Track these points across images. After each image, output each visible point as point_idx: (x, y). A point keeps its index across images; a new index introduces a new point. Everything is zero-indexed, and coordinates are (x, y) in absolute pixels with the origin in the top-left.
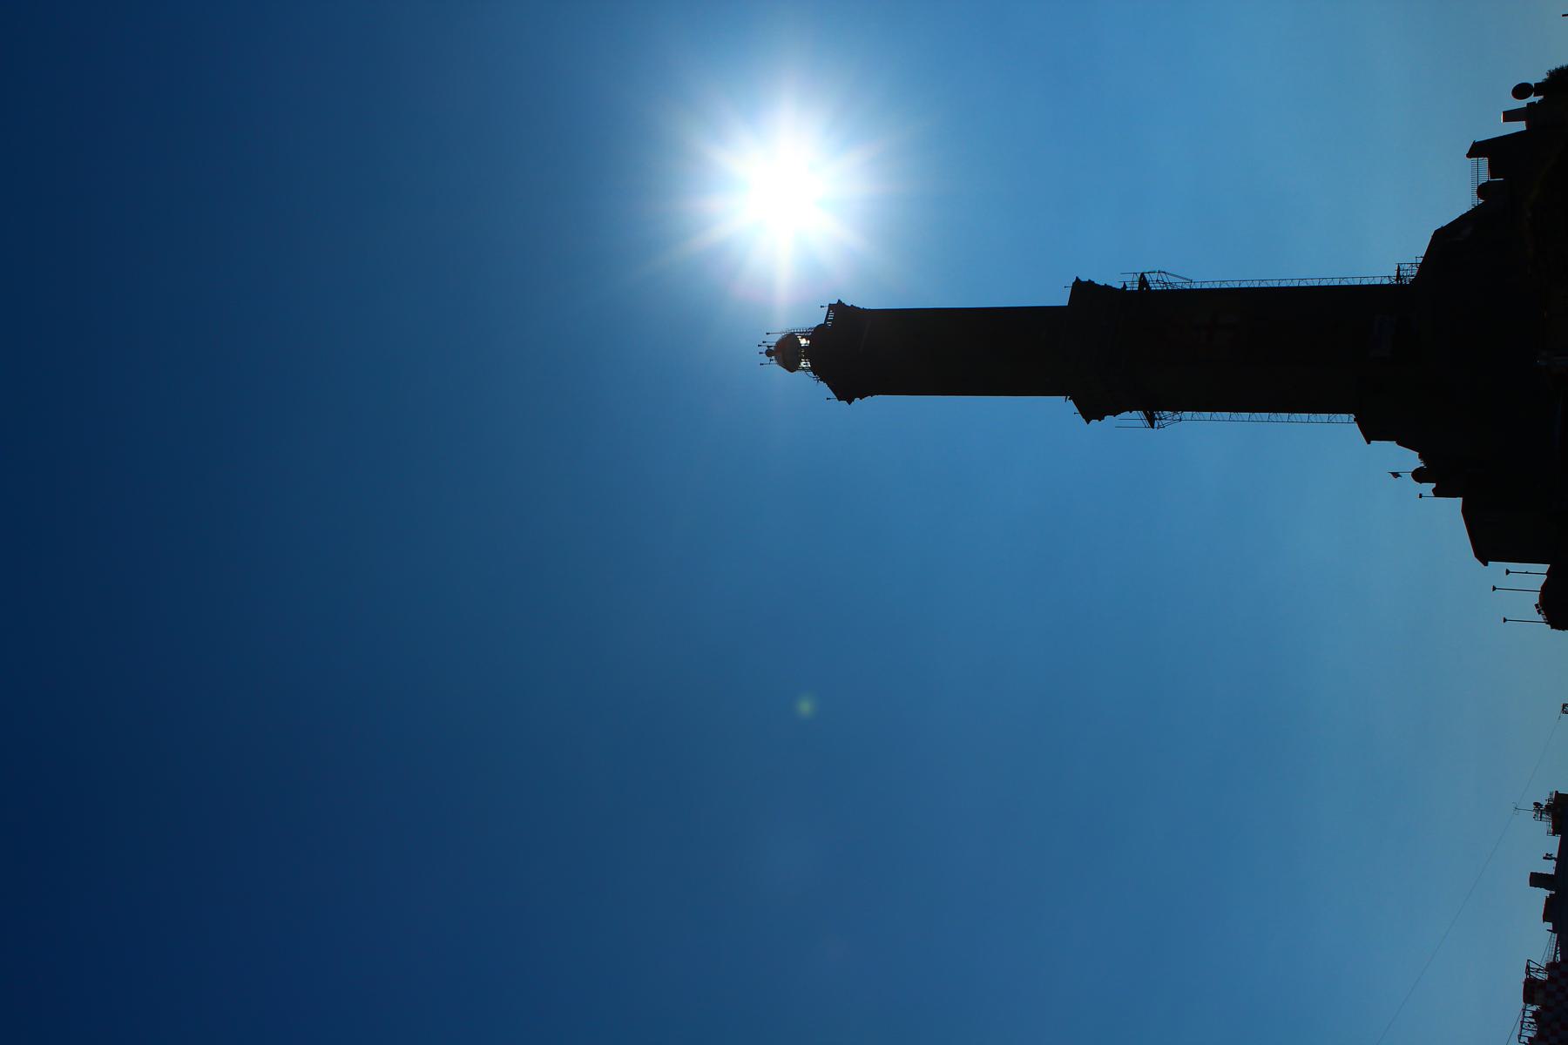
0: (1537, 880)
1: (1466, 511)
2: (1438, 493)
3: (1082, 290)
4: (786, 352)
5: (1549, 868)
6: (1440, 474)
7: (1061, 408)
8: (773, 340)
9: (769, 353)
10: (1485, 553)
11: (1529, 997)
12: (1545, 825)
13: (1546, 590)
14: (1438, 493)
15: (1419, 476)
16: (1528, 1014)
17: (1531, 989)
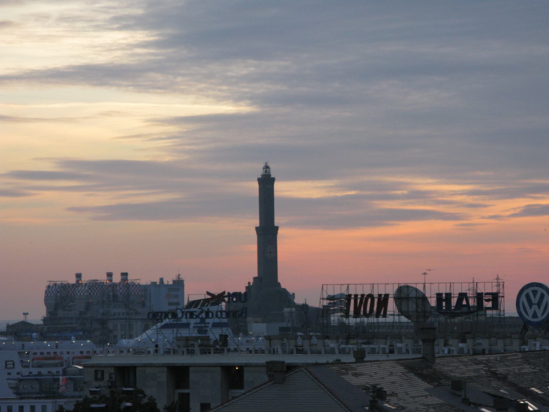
0: (162, 280)
5: (165, 283)
8: (269, 165)
12: (175, 278)
15: (249, 283)
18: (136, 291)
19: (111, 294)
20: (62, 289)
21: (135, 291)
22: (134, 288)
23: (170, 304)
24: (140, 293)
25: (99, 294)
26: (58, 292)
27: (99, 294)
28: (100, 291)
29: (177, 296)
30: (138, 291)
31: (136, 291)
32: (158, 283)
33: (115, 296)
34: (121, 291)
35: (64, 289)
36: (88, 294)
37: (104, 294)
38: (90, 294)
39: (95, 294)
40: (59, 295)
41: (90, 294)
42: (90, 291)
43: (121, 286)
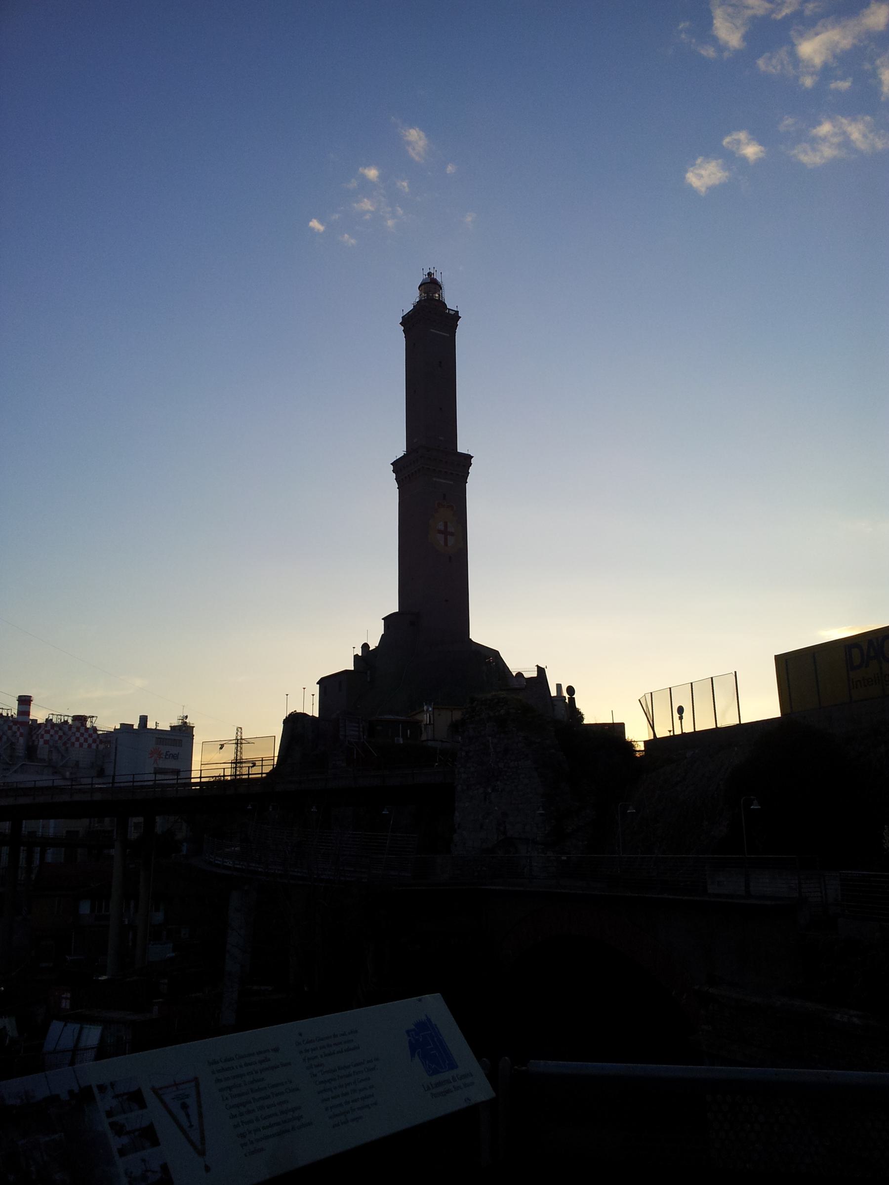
0: (144, 719)
1: (346, 672)
2: (356, 656)
3: (467, 459)
4: (431, 286)
5: (151, 725)
6: (366, 659)
7: (399, 449)
9: (429, 274)
10: (322, 682)
11: (76, 718)
12: (176, 722)
13: (304, 715)
14: (356, 656)
15: (365, 646)
16: (66, 718)
17: (80, 720)
18: (86, 740)
19: (21, 740)
21: (82, 740)
22: (82, 735)
23: (157, 771)
24: (94, 746)
29: (175, 757)
31: (86, 740)
32: (136, 727)
33: (31, 751)
34: (47, 737)
43: (49, 728)
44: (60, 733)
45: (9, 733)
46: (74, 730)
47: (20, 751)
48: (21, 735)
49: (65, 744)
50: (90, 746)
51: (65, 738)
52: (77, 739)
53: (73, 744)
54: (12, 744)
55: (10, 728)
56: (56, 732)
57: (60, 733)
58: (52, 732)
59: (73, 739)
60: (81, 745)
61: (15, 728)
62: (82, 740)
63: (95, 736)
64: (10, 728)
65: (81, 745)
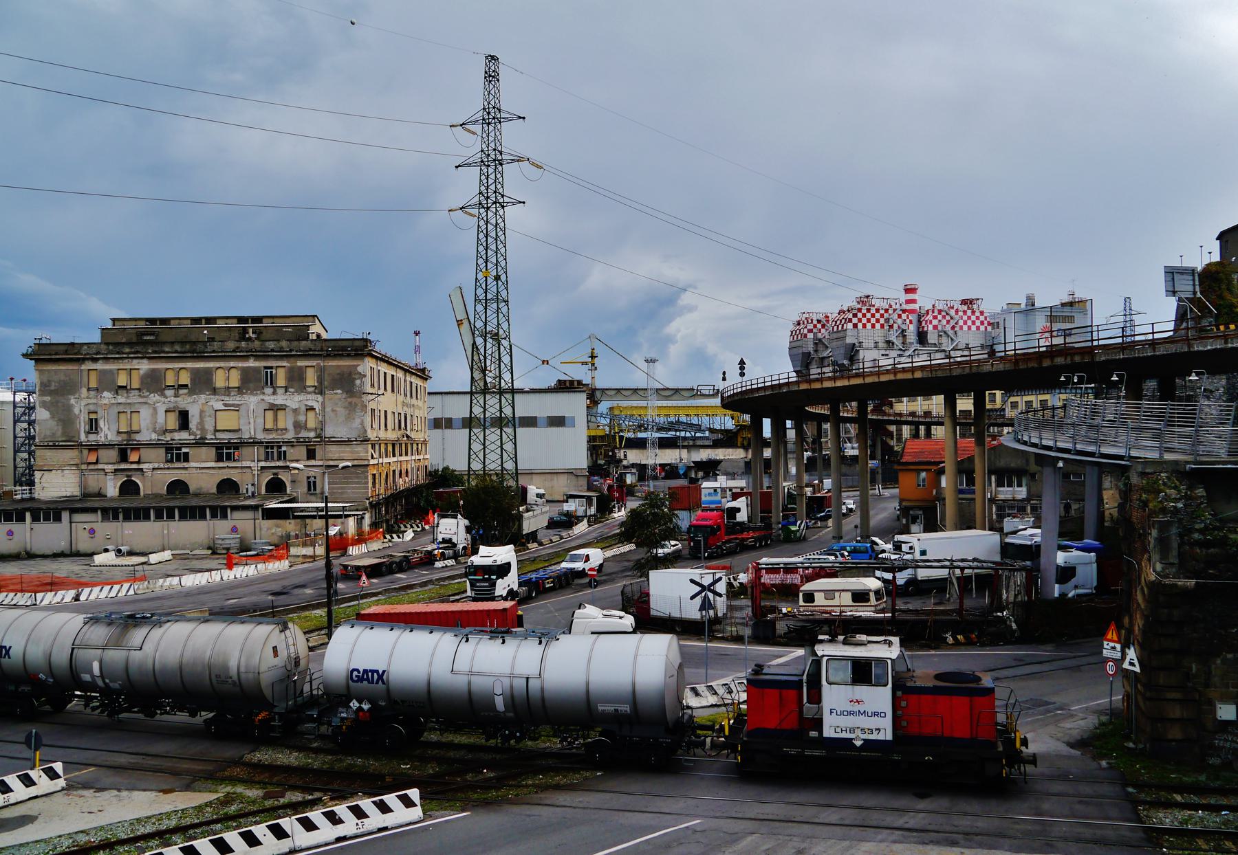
11: (964, 302)
12: (1066, 299)
18: (974, 323)
19: (912, 327)
20: (819, 326)
24: (982, 328)
25: (878, 326)
26: (811, 331)
27: (878, 326)
28: (882, 321)
30: (978, 323)
34: (935, 322)
35: (823, 326)
36: (850, 326)
37: (891, 327)
38: (855, 326)
39: (869, 326)
40: (810, 336)
41: (855, 326)
42: (855, 320)
44: (948, 318)
45: (899, 321)
46: (961, 314)
47: (912, 337)
48: (911, 322)
49: (953, 328)
50: (978, 328)
51: (952, 323)
52: (965, 323)
53: (961, 328)
54: (903, 331)
55: (900, 316)
56: (944, 317)
57: (948, 318)
58: (940, 317)
59: (961, 323)
60: (969, 328)
61: (904, 316)
62: (969, 323)
63: (982, 318)
64: (900, 316)
65: (969, 328)
